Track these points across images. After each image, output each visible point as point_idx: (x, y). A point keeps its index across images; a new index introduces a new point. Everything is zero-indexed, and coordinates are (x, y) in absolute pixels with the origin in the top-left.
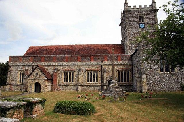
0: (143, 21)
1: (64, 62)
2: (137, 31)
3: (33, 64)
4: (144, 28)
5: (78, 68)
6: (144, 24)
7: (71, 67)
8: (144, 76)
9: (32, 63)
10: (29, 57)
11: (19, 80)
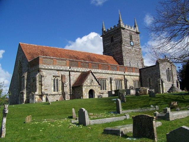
0: (132, 40)
1: (98, 70)
2: (130, 48)
3: (70, 70)
4: (133, 46)
5: (108, 76)
6: (133, 42)
7: (103, 74)
8: (164, 84)
9: (68, 67)
10: (65, 60)
11: (53, 88)
